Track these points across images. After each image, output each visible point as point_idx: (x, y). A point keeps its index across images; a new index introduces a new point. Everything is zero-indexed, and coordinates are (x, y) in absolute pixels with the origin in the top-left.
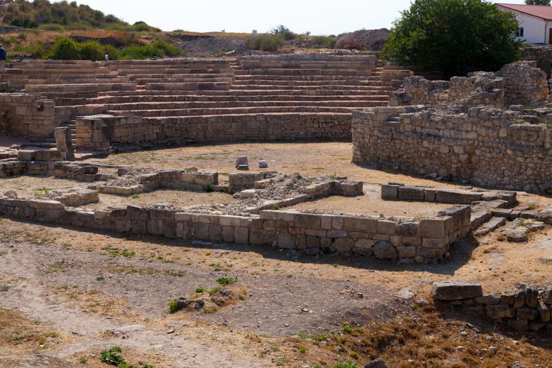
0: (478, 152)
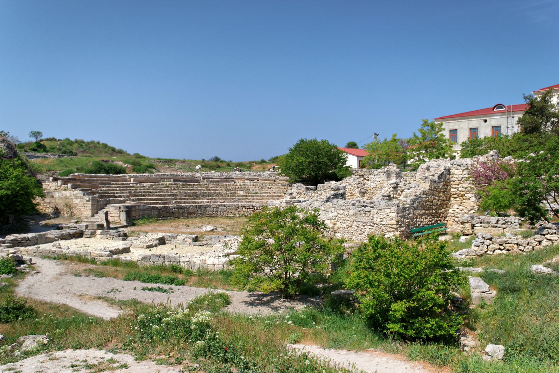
0: (338, 223)
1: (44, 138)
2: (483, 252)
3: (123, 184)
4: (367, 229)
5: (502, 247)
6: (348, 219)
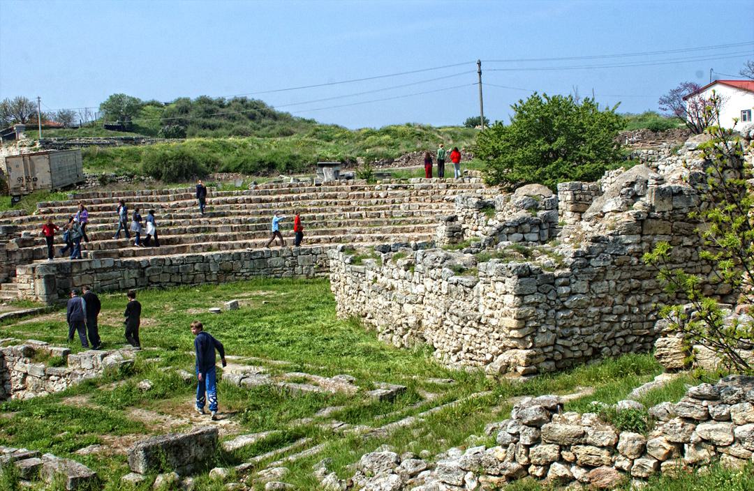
0: (425, 313)
2: (515, 466)
4: (467, 338)
5: (567, 456)
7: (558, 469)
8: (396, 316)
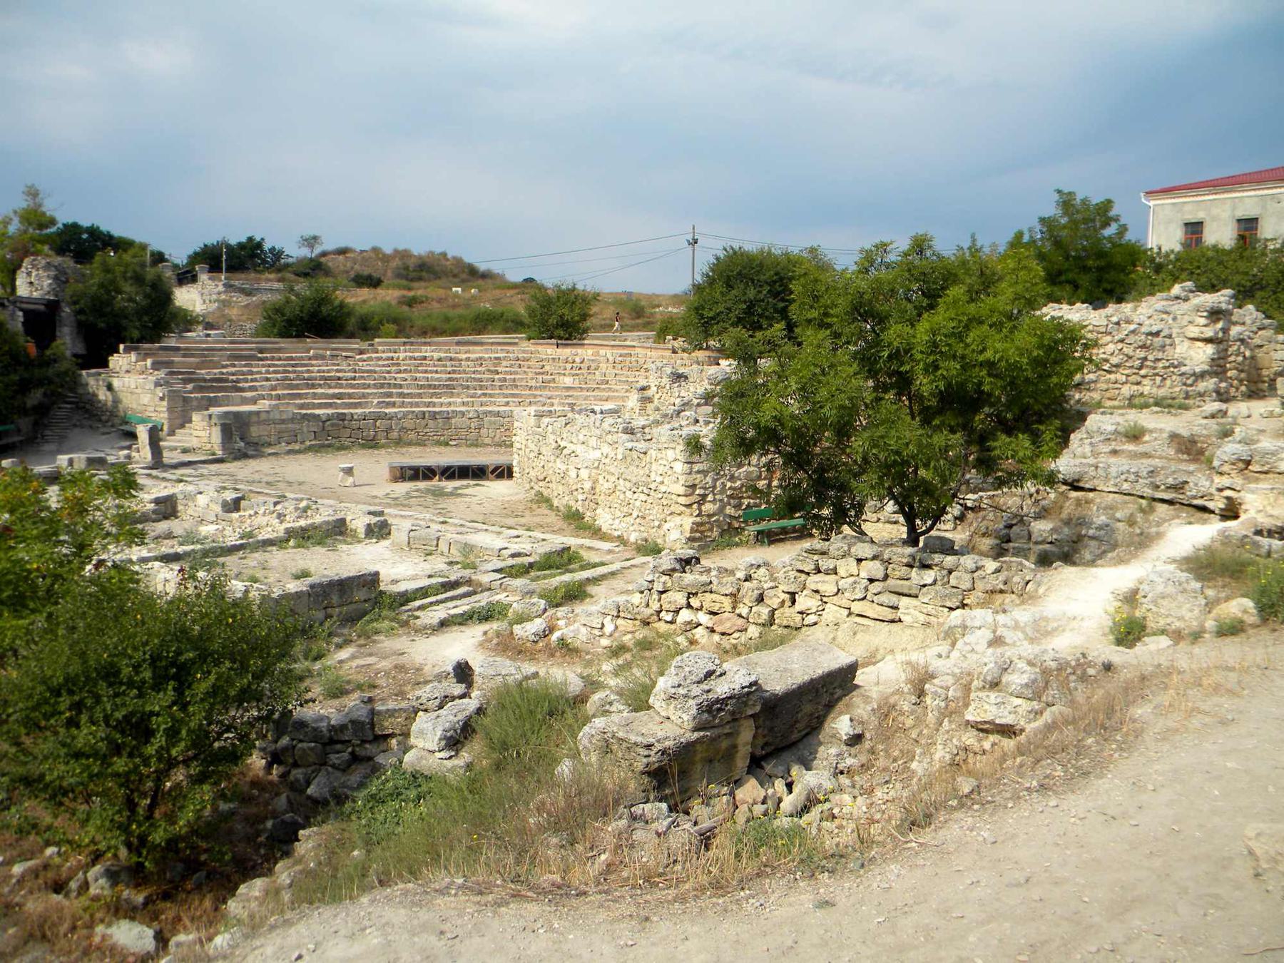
0: (601, 478)
1: (329, 244)
2: (648, 611)
3: (292, 359)
6: (612, 469)
7: (685, 615)
8: (571, 482)
